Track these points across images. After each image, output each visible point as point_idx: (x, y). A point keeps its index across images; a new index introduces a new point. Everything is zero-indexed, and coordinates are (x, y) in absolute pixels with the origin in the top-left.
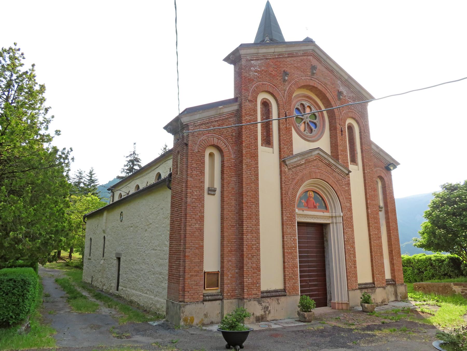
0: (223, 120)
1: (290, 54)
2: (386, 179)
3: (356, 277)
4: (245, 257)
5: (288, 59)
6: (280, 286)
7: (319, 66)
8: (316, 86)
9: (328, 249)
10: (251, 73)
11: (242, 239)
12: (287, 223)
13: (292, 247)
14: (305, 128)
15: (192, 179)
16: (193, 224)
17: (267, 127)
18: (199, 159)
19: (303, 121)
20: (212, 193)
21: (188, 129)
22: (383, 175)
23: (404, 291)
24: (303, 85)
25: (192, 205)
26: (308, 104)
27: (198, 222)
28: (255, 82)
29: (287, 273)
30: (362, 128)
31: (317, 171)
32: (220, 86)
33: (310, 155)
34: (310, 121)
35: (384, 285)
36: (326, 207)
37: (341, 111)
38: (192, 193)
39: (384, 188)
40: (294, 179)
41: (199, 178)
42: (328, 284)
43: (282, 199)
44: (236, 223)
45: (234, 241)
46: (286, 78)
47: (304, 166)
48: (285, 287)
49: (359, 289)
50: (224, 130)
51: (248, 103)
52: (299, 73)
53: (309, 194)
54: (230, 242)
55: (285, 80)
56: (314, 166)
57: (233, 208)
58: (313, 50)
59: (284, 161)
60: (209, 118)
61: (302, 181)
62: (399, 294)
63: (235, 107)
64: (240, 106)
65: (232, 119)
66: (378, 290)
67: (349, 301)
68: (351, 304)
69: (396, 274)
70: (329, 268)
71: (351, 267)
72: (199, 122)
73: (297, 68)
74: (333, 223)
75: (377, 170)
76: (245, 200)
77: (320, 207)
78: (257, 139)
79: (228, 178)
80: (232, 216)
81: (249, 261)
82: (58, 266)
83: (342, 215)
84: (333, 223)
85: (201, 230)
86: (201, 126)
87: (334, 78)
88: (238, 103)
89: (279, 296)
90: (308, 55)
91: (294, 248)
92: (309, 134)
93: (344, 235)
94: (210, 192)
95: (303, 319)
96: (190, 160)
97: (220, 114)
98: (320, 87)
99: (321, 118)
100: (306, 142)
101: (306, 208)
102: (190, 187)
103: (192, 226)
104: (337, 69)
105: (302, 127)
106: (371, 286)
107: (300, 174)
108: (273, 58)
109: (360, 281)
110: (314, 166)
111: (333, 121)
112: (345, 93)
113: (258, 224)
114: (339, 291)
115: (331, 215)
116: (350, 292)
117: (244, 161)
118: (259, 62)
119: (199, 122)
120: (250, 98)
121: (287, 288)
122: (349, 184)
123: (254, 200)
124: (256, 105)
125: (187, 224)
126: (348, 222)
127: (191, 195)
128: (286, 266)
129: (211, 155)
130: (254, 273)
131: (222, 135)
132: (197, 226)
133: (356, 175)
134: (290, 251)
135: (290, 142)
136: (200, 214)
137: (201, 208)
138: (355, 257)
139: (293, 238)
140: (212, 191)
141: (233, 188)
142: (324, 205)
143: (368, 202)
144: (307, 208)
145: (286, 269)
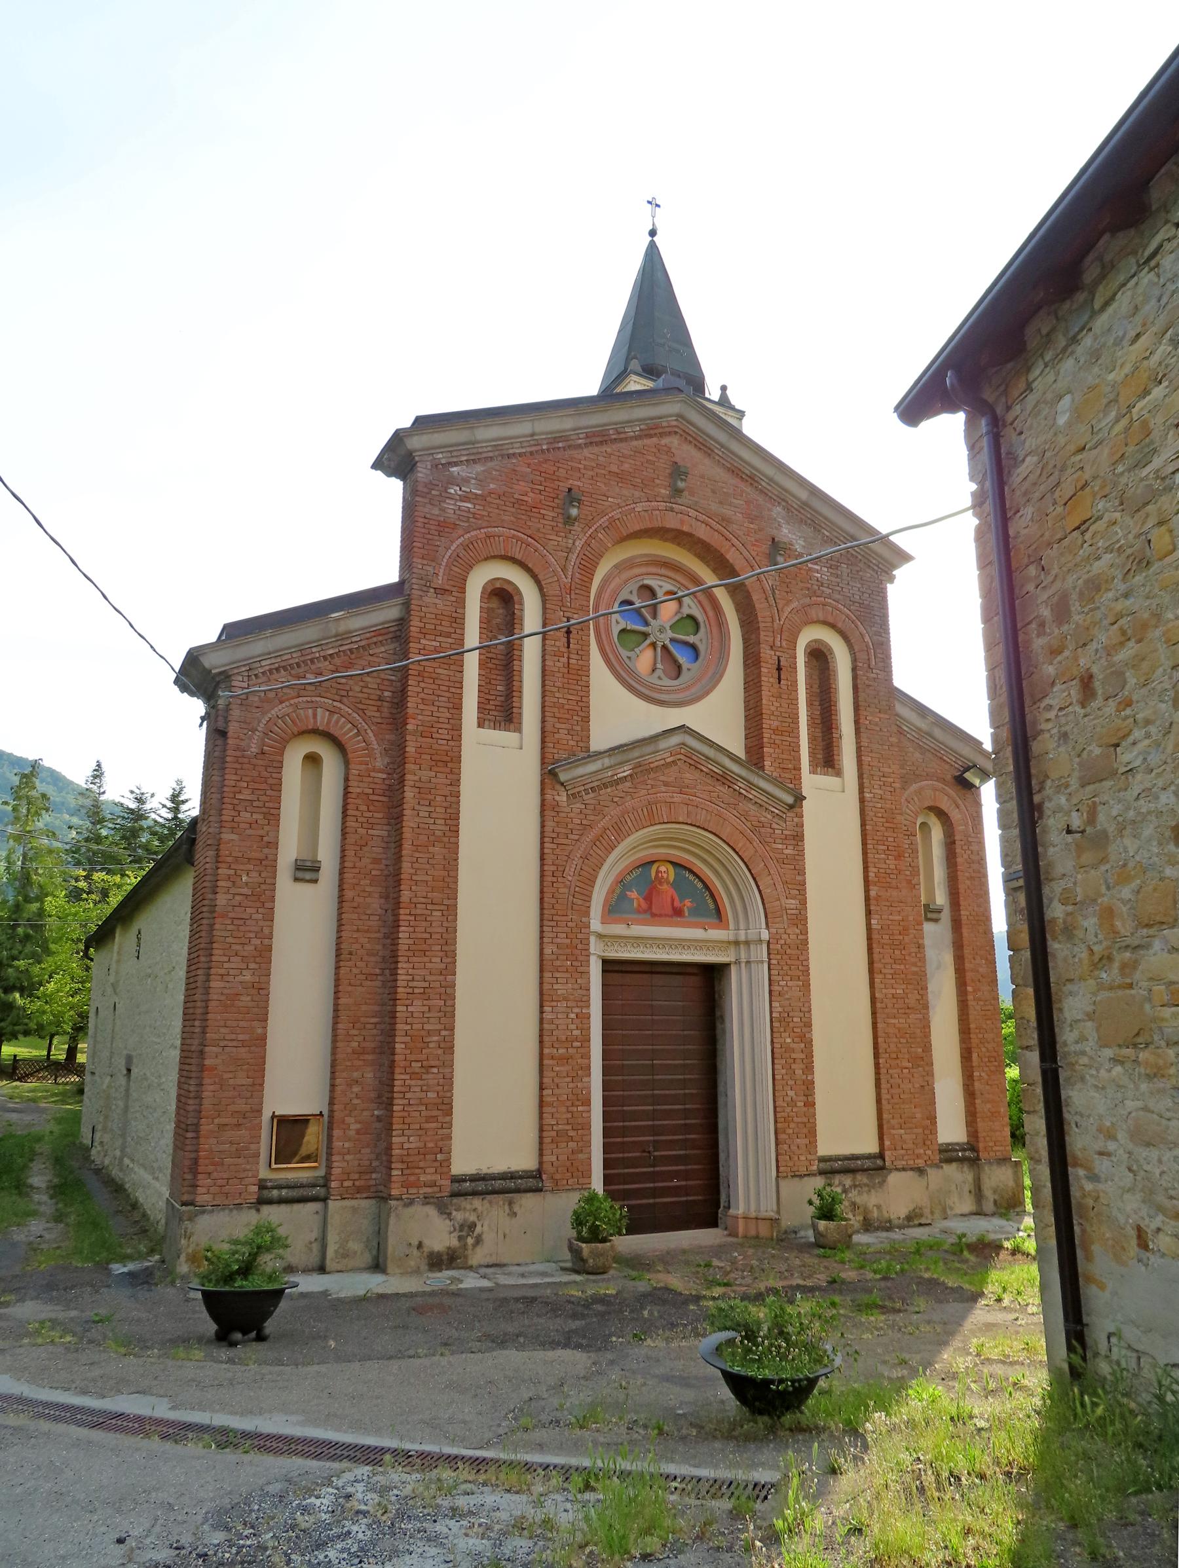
0: (351, 651)
1: (594, 434)
2: (955, 815)
3: (812, 1133)
4: (397, 1070)
5: (586, 452)
6: (523, 1160)
7: (701, 465)
8: (685, 528)
9: (724, 1044)
10: (450, 505)
11: (393, 1015)
12: (558, 963)
13: (569, 1041)
14: (655, 664)
15: (234, 837)
16: (232, 972)
17: (502, 666)
18: (265, 774)
19: (648, 642)
20: (308, 876)
21: (230, 688)
22: (945, 805)
23: (1011, 1183)
24: (637, 528)
25: (231, 915)
26: (668, 587)
27: (252, 966)
28: (461, 532)
29: (548, 1120)
30: (862, 656)
31: (678, 798)
32: (356, 544)
33: (648, 749)
34: (672, 640)
35: (920, 1163)
36: (719, 912)
37: (781, 603)
38: (233, 880)
39: (950, 845)
40: (585, 828)
41: (261, 832)
42: (722, 1156)
43: (542, 892)
44: (383, 965)
45: (373, 1020)
46: (574, 512)
47: (628, 784)
48: (541, 1163)
49: (822, 1173)
50: (351, 682)
51: (430, 598)
52: (625, 492)
53: (658, 872)
54: (357, 1025)
55: (569, 517)
56: (666, 784)
57: (374, 922)
58: (680, 416)
59: (553, 774)
60: (302, 649)
61: (621, 831)
62: (988, 1193)
63: (390, 612)
64: (407, 605)
65: (383, 649)
66: (894, 1178)
67: (778, 1212)
68: (787, 1222)
69: (981, 1125)
70: (726, 1105)
71: (793, 1103)
72: (268, 662)
73: (621, 477)
74: (738, 962)
75: (921, 789)
76: (406, 895)
77: (695, 912)
78: (458, 707)
79: (362, 831)
80: (368, 946)
81: (413, 1082)
82: (56, 1095)
83: (765, 935)
84: (738, 962)
85: (261, 990)
86: (276, 676)
87: (761, 499)
88: (400, 600)
89: (518, 1191)
90: (662, 435)
91: (576, 1044)
92: (666, 682)
93: (771, 1002)
94: (300, 875)
95: (580, 1266)
96: (231, 778)
97: (342, 637)
98: (702, 532)
99: (715, 630)
100: (653, 708)
101: (641, 916)
102: (229, 859)
103: (231, 978)
104: (770, 471)
105: (644, 660)
106: (870, 1168)
107: (614, 812)
108: (531, 453)
109: (827, 1146)
110: (666, 784)
111: (753, 636)
112: (799, 545)
113: (450, 969)
114: (756, 1182)
115: (732, 938)
116: (782, 1183)
117: (408, 777)
118: (479, 468)
119: (268, 662)
120: (439, 581)
121: (547, 1167)
122: (798, 838)
123: (440, 895)
124: (461, 603)
125: (213, 971)
126: (790, 960)
127: (229, 884)
128: (547, 1099)
129: (312, 760)
130: (429, 1119)
131: (345, 700)
132: (248, 977)
133: (830, 811)
134: (561, 1051)
135: (581, 713)
136: (258, 942)
137: (261, 923)
138: (809, 1067)
139: (576, 1010)
140: (306, 870)
141: (376, 861)
142: (712, 906)
143: (873, 893)
144: (648, 916)
145: (545, 1109)
